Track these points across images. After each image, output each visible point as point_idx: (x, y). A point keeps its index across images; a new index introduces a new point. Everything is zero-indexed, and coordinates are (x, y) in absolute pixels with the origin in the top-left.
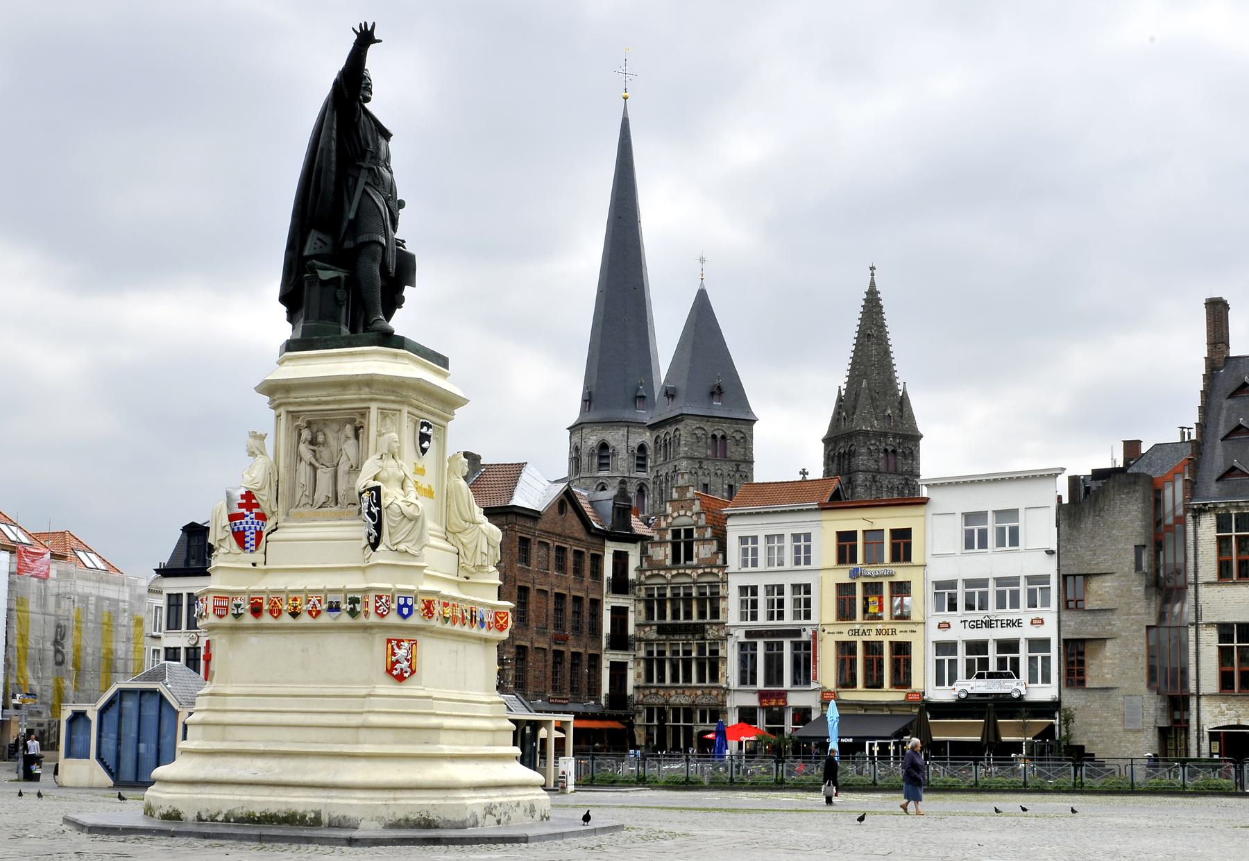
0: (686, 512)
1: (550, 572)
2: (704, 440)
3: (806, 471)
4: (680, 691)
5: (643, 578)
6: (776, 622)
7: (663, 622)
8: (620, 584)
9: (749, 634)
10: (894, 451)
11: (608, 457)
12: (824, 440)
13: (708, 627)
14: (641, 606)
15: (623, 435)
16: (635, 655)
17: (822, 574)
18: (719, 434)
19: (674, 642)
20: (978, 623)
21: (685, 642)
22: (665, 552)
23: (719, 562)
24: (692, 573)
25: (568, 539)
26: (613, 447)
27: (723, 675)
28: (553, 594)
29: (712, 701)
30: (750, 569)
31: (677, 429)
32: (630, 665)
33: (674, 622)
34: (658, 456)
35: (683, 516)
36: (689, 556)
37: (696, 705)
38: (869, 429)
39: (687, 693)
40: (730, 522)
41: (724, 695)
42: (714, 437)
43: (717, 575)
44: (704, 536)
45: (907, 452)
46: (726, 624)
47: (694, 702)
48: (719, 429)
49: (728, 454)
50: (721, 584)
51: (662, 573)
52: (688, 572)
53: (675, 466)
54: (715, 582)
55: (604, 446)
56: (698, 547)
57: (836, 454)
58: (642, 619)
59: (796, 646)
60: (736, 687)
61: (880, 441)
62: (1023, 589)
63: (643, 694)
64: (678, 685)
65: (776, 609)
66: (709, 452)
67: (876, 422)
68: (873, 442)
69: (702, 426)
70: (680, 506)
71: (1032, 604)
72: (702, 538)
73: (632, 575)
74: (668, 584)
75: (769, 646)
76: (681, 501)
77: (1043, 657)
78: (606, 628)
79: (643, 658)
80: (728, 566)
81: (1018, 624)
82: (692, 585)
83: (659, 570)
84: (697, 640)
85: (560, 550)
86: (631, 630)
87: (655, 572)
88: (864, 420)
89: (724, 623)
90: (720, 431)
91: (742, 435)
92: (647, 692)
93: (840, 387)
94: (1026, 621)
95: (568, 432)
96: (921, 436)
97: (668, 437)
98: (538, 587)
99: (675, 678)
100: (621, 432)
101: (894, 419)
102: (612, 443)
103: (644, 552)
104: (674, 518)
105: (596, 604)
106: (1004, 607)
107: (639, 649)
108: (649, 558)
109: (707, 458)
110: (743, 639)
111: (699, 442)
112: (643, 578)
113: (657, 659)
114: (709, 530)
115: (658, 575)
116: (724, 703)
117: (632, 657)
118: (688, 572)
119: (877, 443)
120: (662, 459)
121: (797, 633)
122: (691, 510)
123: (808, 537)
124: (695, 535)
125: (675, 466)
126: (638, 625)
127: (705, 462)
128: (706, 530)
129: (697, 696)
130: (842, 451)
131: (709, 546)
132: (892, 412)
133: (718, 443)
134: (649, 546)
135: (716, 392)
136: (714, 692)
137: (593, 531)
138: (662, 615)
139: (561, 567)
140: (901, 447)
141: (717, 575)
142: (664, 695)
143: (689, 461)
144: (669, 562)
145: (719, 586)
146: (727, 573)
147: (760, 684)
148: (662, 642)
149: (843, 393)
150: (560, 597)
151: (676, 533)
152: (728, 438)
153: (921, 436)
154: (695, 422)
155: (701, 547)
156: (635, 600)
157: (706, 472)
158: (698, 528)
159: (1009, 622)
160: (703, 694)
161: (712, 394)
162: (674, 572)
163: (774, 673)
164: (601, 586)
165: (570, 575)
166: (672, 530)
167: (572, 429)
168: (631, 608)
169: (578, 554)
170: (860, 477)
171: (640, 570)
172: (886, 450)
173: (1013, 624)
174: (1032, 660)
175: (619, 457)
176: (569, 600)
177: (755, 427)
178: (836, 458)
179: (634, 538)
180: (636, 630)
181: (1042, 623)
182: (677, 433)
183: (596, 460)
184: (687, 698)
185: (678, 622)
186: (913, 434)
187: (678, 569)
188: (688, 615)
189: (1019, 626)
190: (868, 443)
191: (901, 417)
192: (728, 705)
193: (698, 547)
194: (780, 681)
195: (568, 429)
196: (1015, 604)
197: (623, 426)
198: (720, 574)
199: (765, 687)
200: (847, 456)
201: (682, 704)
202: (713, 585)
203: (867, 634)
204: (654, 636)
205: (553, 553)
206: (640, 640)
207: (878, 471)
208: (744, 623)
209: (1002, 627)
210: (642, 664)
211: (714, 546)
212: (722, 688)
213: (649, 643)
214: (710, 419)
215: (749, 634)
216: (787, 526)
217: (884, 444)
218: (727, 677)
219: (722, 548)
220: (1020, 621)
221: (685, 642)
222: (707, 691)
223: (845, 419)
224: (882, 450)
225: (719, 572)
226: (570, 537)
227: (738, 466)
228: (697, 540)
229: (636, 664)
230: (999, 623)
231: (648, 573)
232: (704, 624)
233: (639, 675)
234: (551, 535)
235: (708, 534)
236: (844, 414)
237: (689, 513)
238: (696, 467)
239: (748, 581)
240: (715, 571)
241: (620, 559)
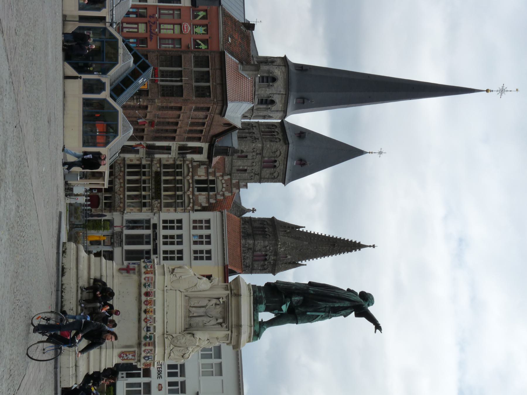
0: (224, 188)
1: (190, 120)
2: (273, 156)
3: (255, 212)
4: (122, 185)
5: (187, 162)
6: (162, 240)
7: (162, 175)
8: (183, 150)
9: (155, 226)
10: (266, 260)
11: (267, 82)
12: (273, 218)
13: (159, 201)
14: (171, 162)
15: (280, 91)
16: (143, 158)
18: (277, 164)
19: (150, 181)
20: (160, 368)
21: (151, 188)
22: (202, 175)
23: (196, 207)
24: (190, 191)
25: (209, 128)
26: (273, 86)
27: (132, 210)
28: (177, 121)
29: (116, 204)
30: (192, 225)
31: (280, 140)
32: (137, 156)
33: (162, 181)
34: (265, 127)
35: (223, 186)
36: (200, 190)
37: (114, 194)
38: (279, 246)
39: (122, 189)
40: (218, 214)
41: (120, 211)
42: (275, 161)
43: (189, 206)
44: (211, 198)
45: (265, 267)
46: (160, 212)
47: (116, 193)
48: (280, 164)
49: (265, 169)
50: (183, 208)
51: (190, 174)
52: (191, 189)
53: (258, 139)
54: (184, 205)
55: (274, 80)
56: (204, 195)
57: (265, 226)
58: (164, 162)
59: (148, 252)
61: (271, 252)
62: (178, 379)
63: (120, 163)
64: (126, 184)
65: (169, 240)
66: (266, 159)
67: (282, 250)
68: (271, 248)
69: (282, 155)
70: (228, 184)
71: (170, 384)
72: (210, 197)
73: (189, 156)
74: (184, 177)
75: (148, 236)
76: (231, 185)
77: (140, 390)
78: (158, 144)
79: (141, 163)
80: (193, 212)
81: (159, 377)
82: (183, 192)
83: (192, 172)
84: (152, 195)
85: (203, 124)
86: (157, 156)
87: (191, 170)
88: (284, 244)
89: (161, 210)
90: (278, 165)
91: (276, 177)
92: (122, 165)
93: (305, 227)
94: (161, 381)
95: (283, 56)
96: (274, 275)
97: (275, 134)
98: (182, 115)
99: (130, 182)
100: (282, 90)
101: (285, 259)
102: (276, 84)
103: (202, 163)
104: (221, 180)
105: (173, 139)
106: (168, 369)
107: (147, 161)
108: (199, 166)
109: (263, 157)
110: (152, 222)
111: (272, 153)
112: (187, 162)
113: (141, 171)
114: (214, 201)
115: (189, 172)
116: (116, 211)
117: (142, 156)
118: (191, 189)
119: (270, 251)
120: (263, 130)
121: (155, 252)
122: (226, 191)
123: (209, 258)
124: (211, 193)
125: (258, 139)
126: (160, 160)
127: (259, 157)
128: (214, 200)
129: (120, 195)
130: (267, 230)
131: (205, 202)
132: (289, 259)
133: (271, 164)
134: (205, 166)
135: (302, 162)
136: (122, 205)
137: (214, 138)
138: (166, 174)
139: (192, 124)
140: (269, 264)
141: (189, 206)
142: (120, 176)
143: (261, 148)
144: (196, 178)
145: (183, 207)
146: (189, 212)
147: (126, 232)
148: (150, 174)
149: (301, 229)
150: (177, 124)
151: (213, 182)
152: (274, 169)
153: (274, 275)
154: (284, 151)
155: (204, 196)
156: (175, 158)
157: (255, 157)
158: (216, 195)
159: (160, 372)
160: (121, 198)
161: (301, 160)
162: (191, 181)
163: (133, 240)
164: (183, 141)
165: (188, 128)
166: (214, 180)
167: (285, 59)
168: (170, 156)
169: (201, 131)
170: (251, 242)
171: (192, 161)
172: (266, 255)
173: (159, 374)
174: (139, 385)
175: (267, 89)
176: (175, 128)
177: (280, 184)
178: (262, 226)
179: (210, 157)
180: (158, 159)
181: (160, 390)
182: (278, 140)
183: (265, 75)
184: (118, 189)
185: (162, 184)
186: (276, 270)
187: (192, 183)
188: (166, 190)
189: (158, 377)
190: (271, 246)
191: (286, 263)
192: (115, 213)
193: (204, 195)
194: (128, 243)
195: (285, 56)
196: (170, 375)
197: (286, 91)
198: (189, 208)
199: (125, 235)
200: (263, 233)
201: (115, 186)
202: (182, 204)
204: (154, 169)
205: (201, 121)
206: (152, 161)
207: (254, 251)
208: (161, 222)
209: (158, 368)
210: (138, 162)
211: (205, 204)
212: (124, 210)
213: (150, 166)
214: (286, 159)
215: (155, 226)
216: (215, 247)
217: (270, 254)
218: (130, 213)
219: (204, 209)
220: (160, 378)
221: (151, 188)
222: (122, 201)
223: (286, 231)
224: (266, 253)
225: (190, 207)
226: (210, 128)
227: (258, 174)
228: (209, 195)
229: (138, 159)
230: (160, 366)
231: (190, 166)
232: (161, 199)
233: (131, 160)
234: (211, 120)
235: (212, 201)
236: (288, 231)
237: (224, 189)
238: (257, 151)
239: (185, 224)
240: (191, 205)
241: (199, 150)
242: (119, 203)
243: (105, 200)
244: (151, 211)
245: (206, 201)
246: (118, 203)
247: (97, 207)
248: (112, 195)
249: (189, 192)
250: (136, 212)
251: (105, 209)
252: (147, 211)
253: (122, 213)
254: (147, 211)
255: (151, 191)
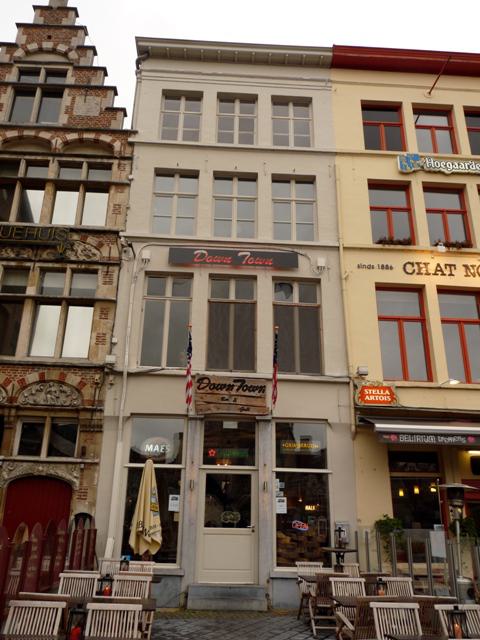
13: (76, 237)
17: (338, 160)
21: (13, 264)
29: (63, 400)
37: (18, 408)
44: (89, 81)
47: (12, 399)
50: (116, 162)
56: (74, 99)
60: (135, 368)
116: (96, 407)
129: (24, 386)
145: (111, 164)
146: (132, 144)
147: (199, 364)
160: (42, 381)
192: (109, 410)
193: (74, 99)
194: (248, 360)
203: (447, 272)
221: (13, 264)
242: (65, 388)
243: (38, 453)
244: (116, 269)
245: (98, 96)
246: (61, 392)
247: (66, 487)
248: (18, 417)
249: (53, 141)
250: (110, 321)
251: (83, 453)
252: (111, 283)
253: (111, 378)
254: (111, 283)
255: (28, 264)
